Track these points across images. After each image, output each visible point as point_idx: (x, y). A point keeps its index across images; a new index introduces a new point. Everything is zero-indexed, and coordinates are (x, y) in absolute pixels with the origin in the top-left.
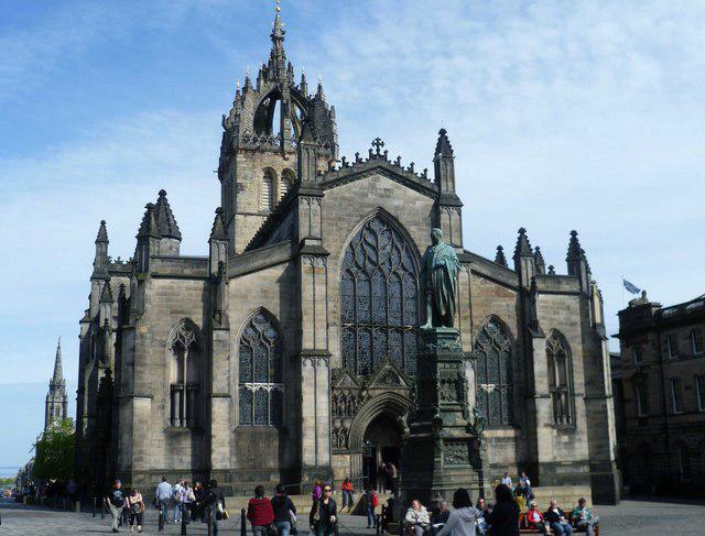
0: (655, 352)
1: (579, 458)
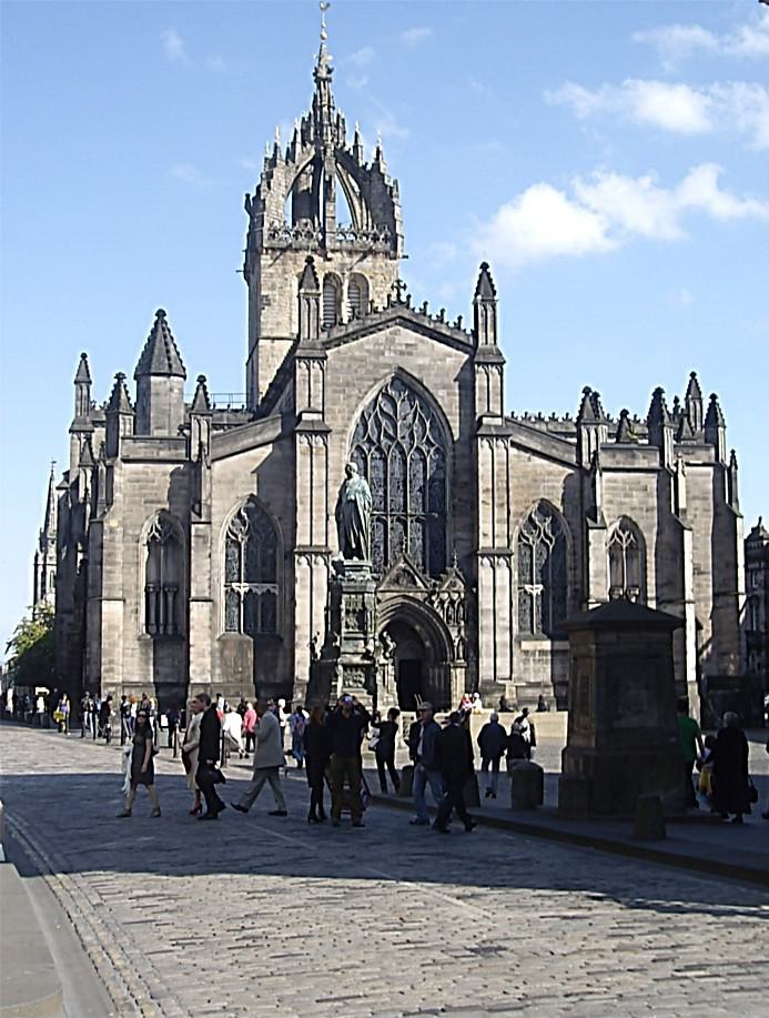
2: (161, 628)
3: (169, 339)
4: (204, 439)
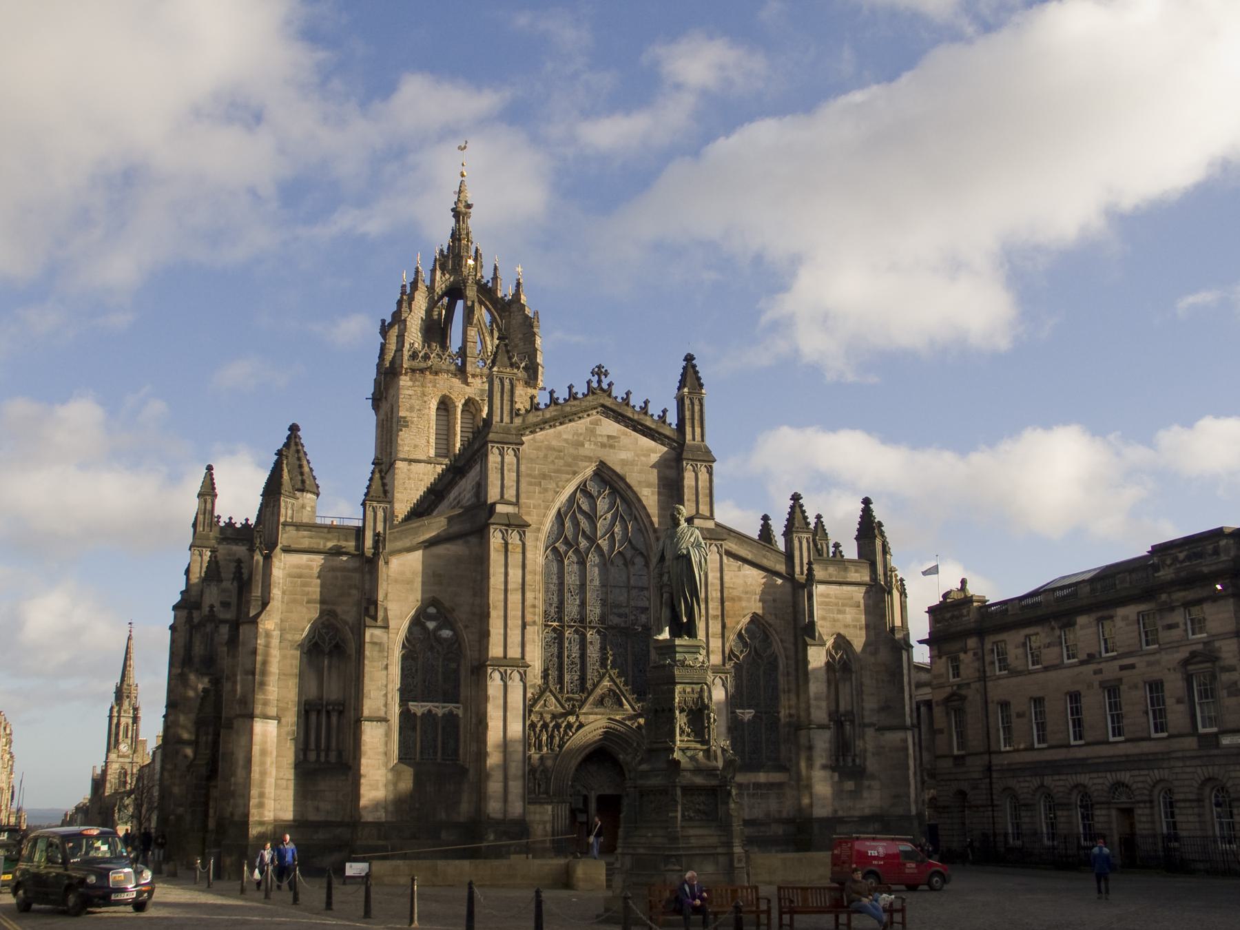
0: (976, 664)
1: (867, 812)
2: (323, 754)
3: (302, 454)
4: (380, 528)
